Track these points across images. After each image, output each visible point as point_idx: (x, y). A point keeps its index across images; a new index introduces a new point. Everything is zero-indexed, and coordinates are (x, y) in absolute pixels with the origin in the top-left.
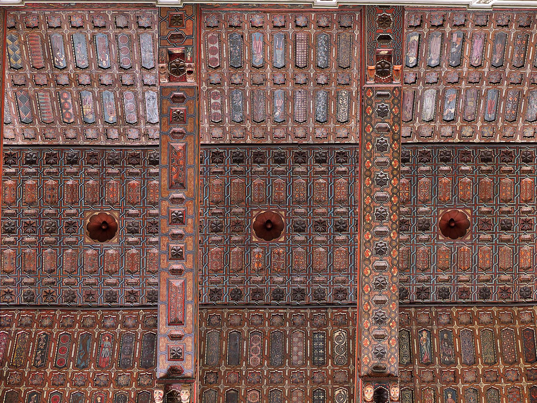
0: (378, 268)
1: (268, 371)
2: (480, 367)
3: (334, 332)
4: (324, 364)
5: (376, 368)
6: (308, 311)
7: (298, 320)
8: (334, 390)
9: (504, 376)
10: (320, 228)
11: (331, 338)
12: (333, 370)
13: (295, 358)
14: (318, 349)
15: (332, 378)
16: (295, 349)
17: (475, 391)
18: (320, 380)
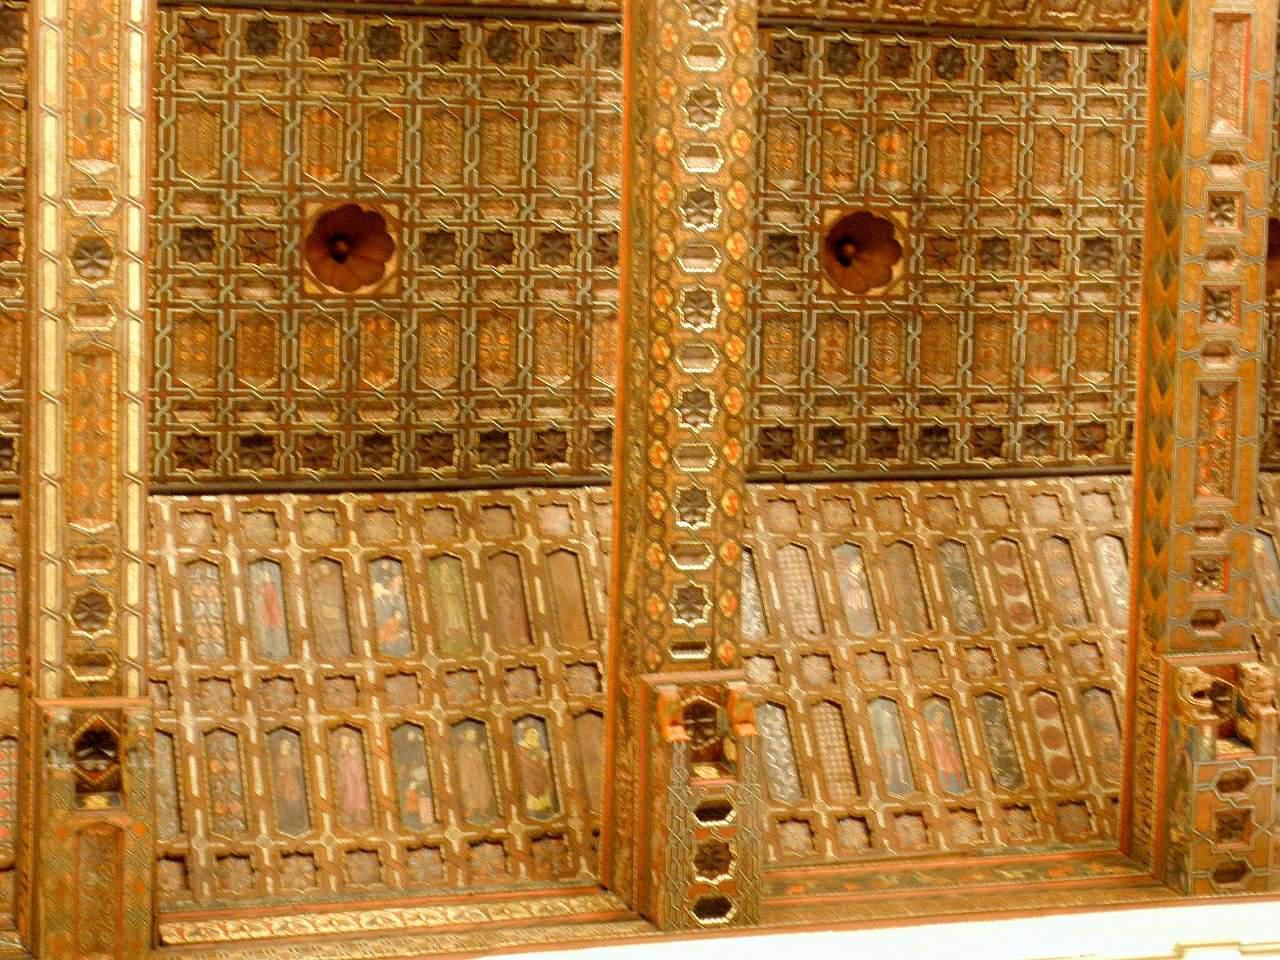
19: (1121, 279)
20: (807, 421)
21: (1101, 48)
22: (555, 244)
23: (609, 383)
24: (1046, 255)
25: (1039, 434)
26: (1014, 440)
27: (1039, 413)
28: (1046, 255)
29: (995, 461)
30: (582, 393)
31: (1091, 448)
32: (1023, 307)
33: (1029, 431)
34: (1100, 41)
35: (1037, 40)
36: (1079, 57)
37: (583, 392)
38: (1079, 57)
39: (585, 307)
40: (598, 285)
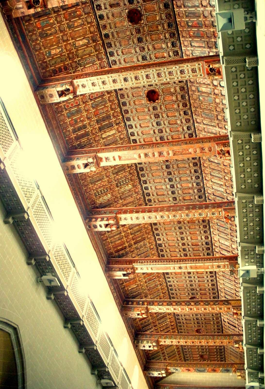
0: (156, 216)
1: (110, 171)
2: (129, 231)
3: (131, 184)
4: (117, 186)
5: (121, 218)
6: (136, 173)
7: (132, 171)
8: (109, 194)
9: (128, 238)
10: (169, 174)
11: (127, 185)
12: (116, 191)
13: (117, 177)
14: (123, 182)
15: (113, 191)
16: (121, 175)
17: (121, 233)
18: (111, 188)
19: (162, 120)
20: (192, 161)
21: (128, 128)
22: (173, 193)
23: (190, 185)
24: (161, 131)
25: (189, 128)
26: (190, 132)
27: (185, 128)
28: (161, 131)
29: (194, 134)
30: (192, 188)
31: (189, 120)
32: (169, 134)
33: (188, 130)
34: (127, 128)
35: (129, 137)
36: (130, 131)
37: (192, 188)
38: (130, 131)
39: (180, 189)
40: (177, 187)
